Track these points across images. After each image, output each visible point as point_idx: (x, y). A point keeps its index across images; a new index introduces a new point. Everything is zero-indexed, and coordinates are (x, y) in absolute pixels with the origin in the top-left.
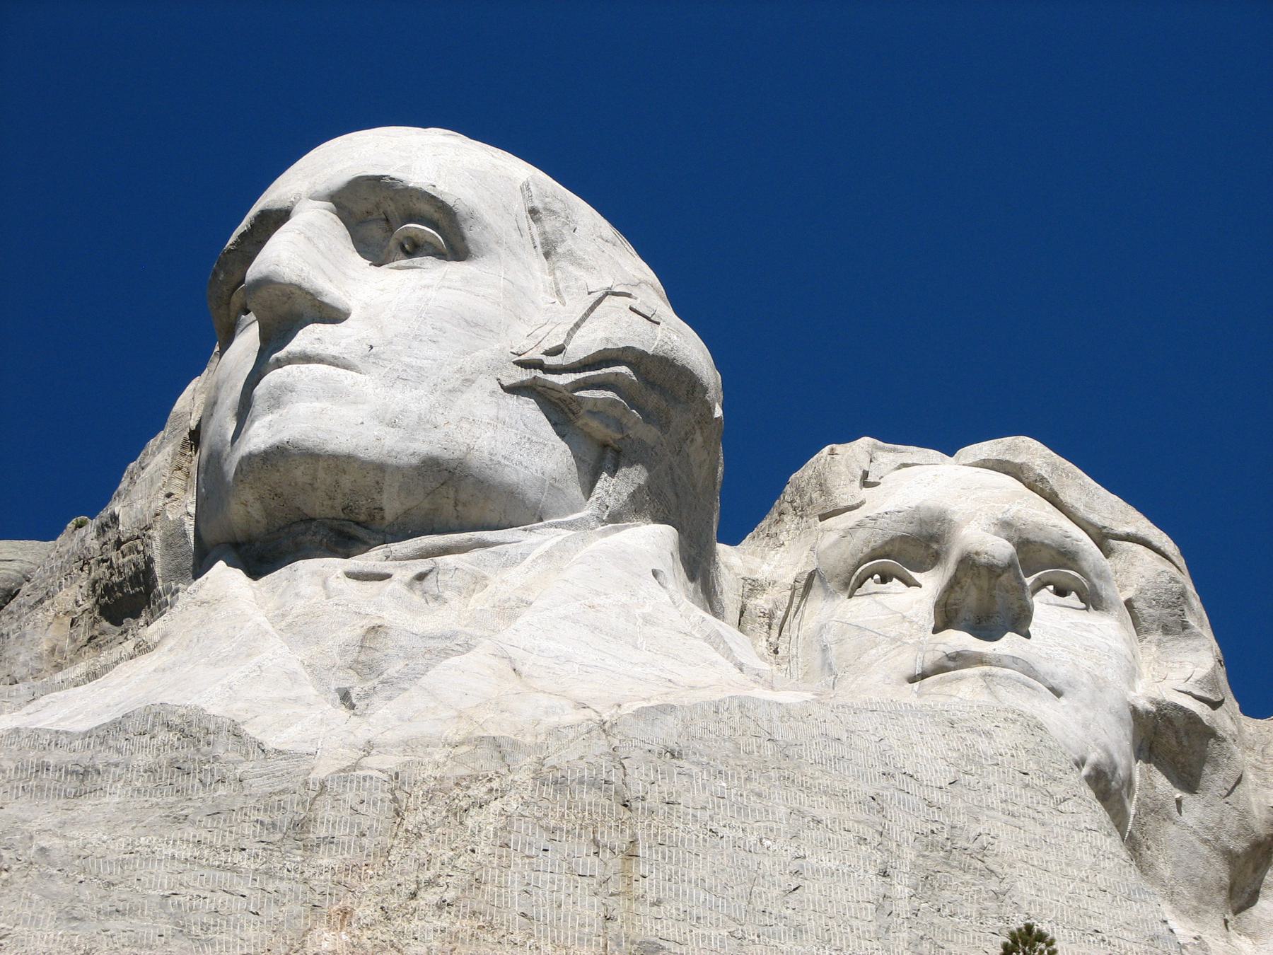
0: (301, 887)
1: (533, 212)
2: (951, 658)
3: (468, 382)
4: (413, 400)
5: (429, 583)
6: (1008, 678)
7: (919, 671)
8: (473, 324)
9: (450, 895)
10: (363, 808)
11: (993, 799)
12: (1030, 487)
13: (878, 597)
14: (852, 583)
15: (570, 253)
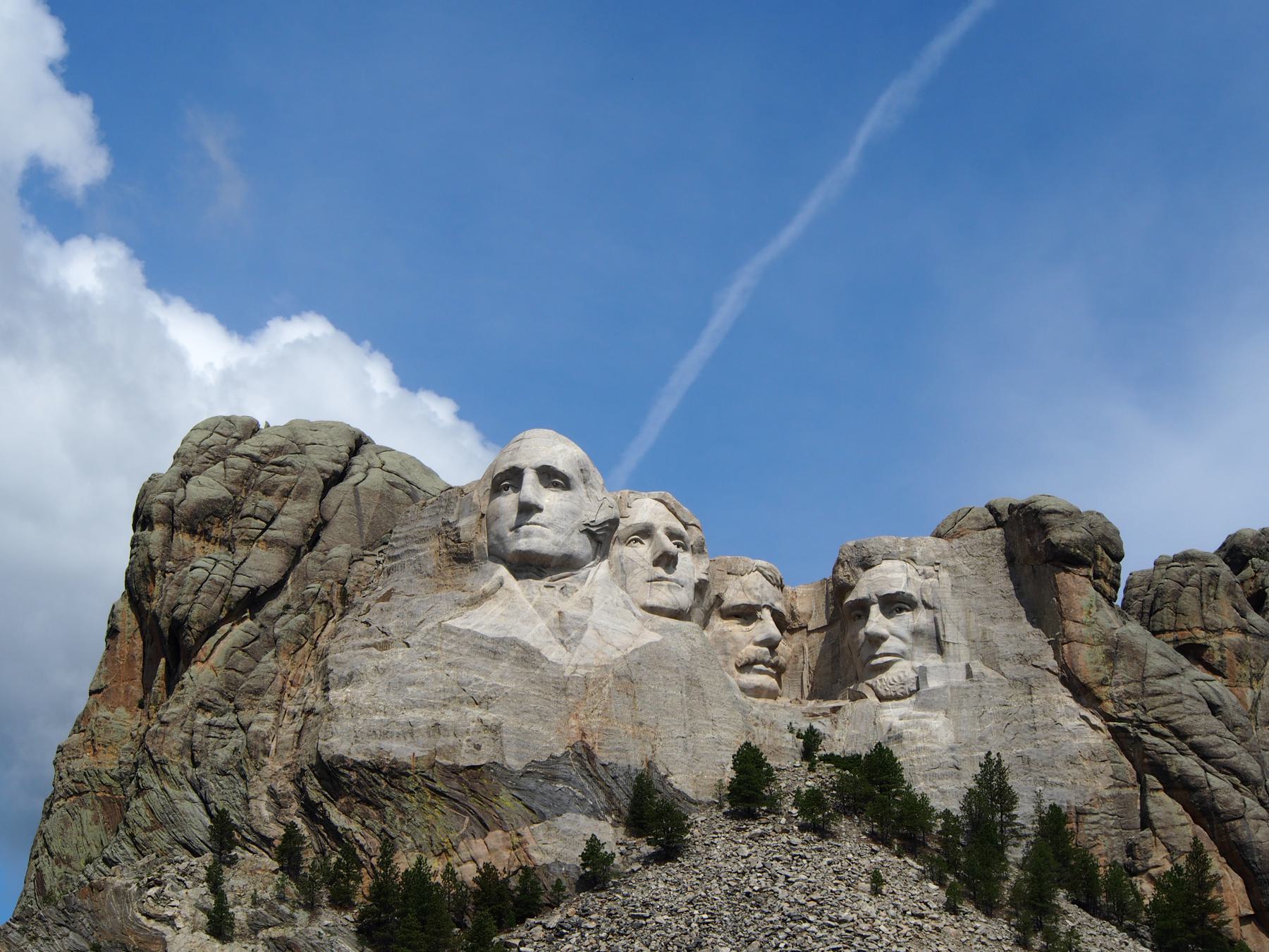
4: (561, 538)
8: (574, 514)
14: (627, 542)
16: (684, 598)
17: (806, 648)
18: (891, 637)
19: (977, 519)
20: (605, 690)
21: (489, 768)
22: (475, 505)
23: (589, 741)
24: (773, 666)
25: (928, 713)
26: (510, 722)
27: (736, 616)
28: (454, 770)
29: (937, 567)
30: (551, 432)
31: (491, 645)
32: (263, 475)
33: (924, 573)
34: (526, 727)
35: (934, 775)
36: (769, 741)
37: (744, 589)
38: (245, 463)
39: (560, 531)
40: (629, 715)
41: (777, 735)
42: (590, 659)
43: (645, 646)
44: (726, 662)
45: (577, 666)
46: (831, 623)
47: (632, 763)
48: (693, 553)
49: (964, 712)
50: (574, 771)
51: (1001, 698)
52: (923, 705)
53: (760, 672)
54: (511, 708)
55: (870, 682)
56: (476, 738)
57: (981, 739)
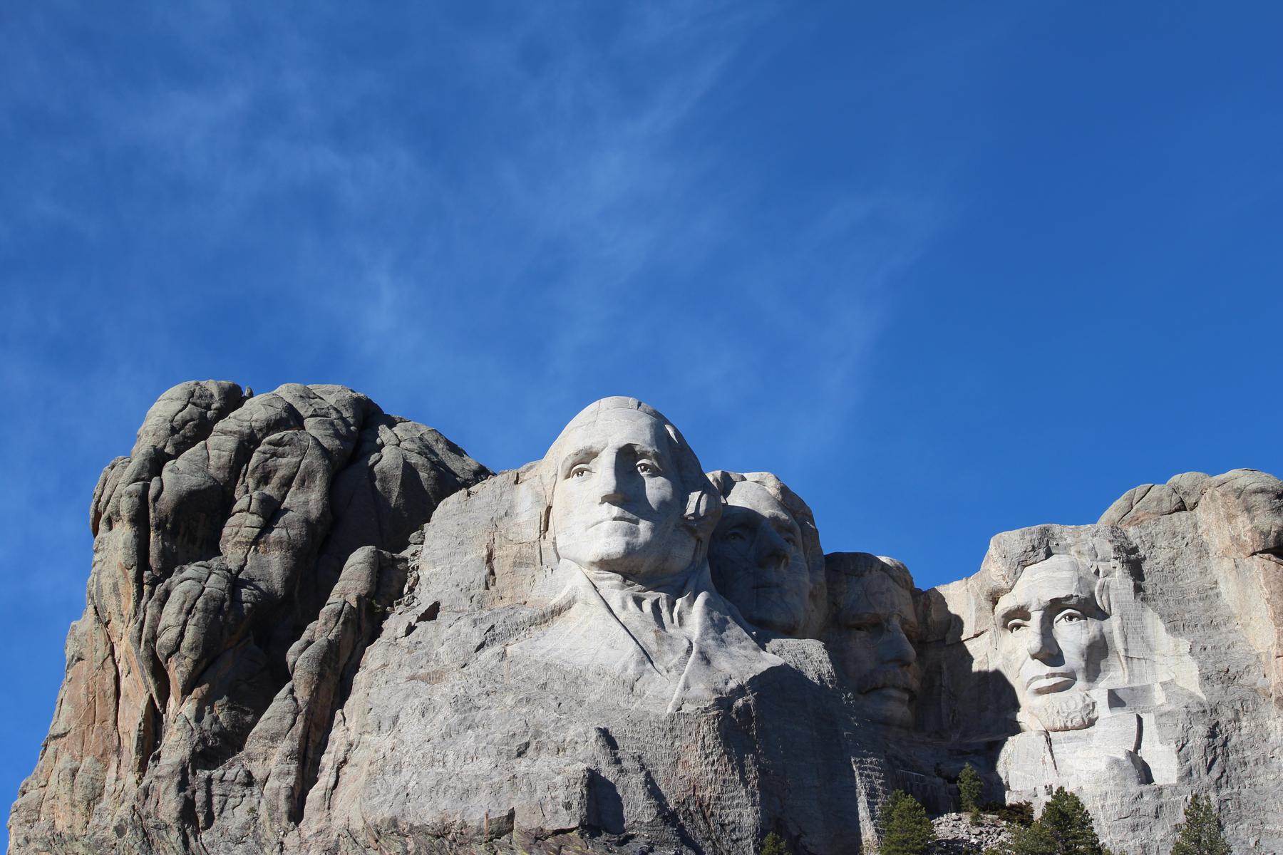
17: (944, 667)
19: (1160, 500)
22: (537, 494)
24: (907, 690)
27: (859, 629)
28: (539, 837)
29: (1113, 563)
30: (632, 401)
32: (255, 458)
33: (1097, 572)
38: (230, 443)
49: (1159, 747)
51: (1201, 729)
53: (890, 698)
54: (606, 754)
57: (1181, 779)
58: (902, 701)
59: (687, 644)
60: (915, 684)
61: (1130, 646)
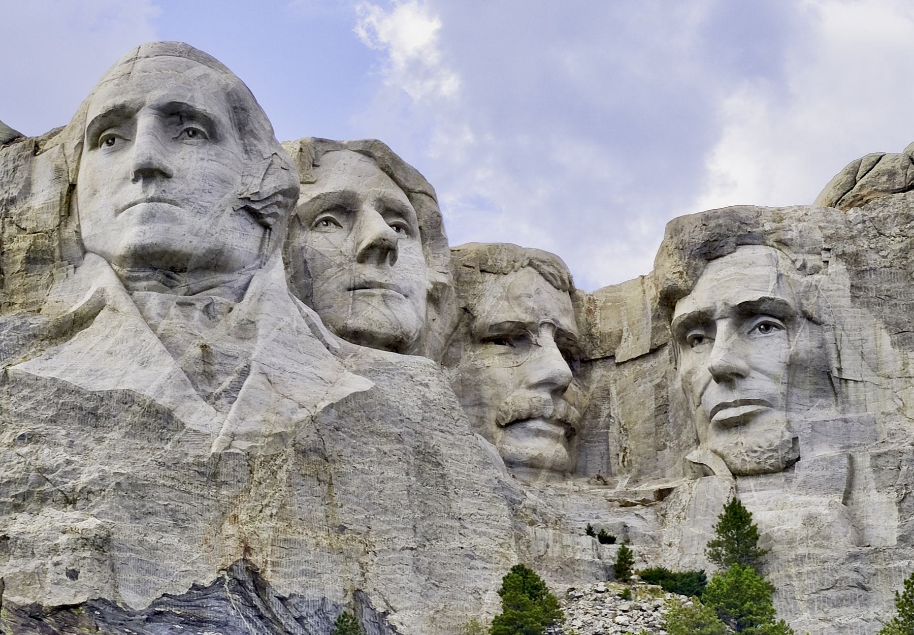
0: (218, 504)
1: (235, 108)
2: (366, 282)
3: (223, 211)
4: (202, 223)
5: (211, 308)
6: (392, 296)
7: (352, 286)
8: (224, 182)
9: (274, 511)
10: (237, 468)
11: (435, 425)
12: (383, 169)
13: (326, 235)
14: (314, 225)
15: (252, 131)
16: (409, 315)
17: (613, 391)
18: (754, 374)
19: (892, 174)
20: (282, 475)
21: (92, 609)
23: (256, 559)
25: (815, 499)
26: (127, 531)
27: (499, 341)
29: (825, 256)
31: (91, 405)
33: (804, 266)
34: (152, 539)
35: (826, 600)
36: (555, 551)
37: (511, 297)
39: (201, 211)
40: (321, 515)
41: (567, 539)
42: (254, 422)
43: (346, 400)
44: (481, 420)
45: (233, 436)
46: (654, 351)
47: (328, 595)
48: (424, 241)
49: (875, 496)
50: (230, 608)
52: (806, 486)
53: (539, 433)
55: (720, 449)
56: (66, 559)
57: (902, 539)
58: (556, 438)
59: (242, 365)
60: (574, 415)
61: (844, 365)
